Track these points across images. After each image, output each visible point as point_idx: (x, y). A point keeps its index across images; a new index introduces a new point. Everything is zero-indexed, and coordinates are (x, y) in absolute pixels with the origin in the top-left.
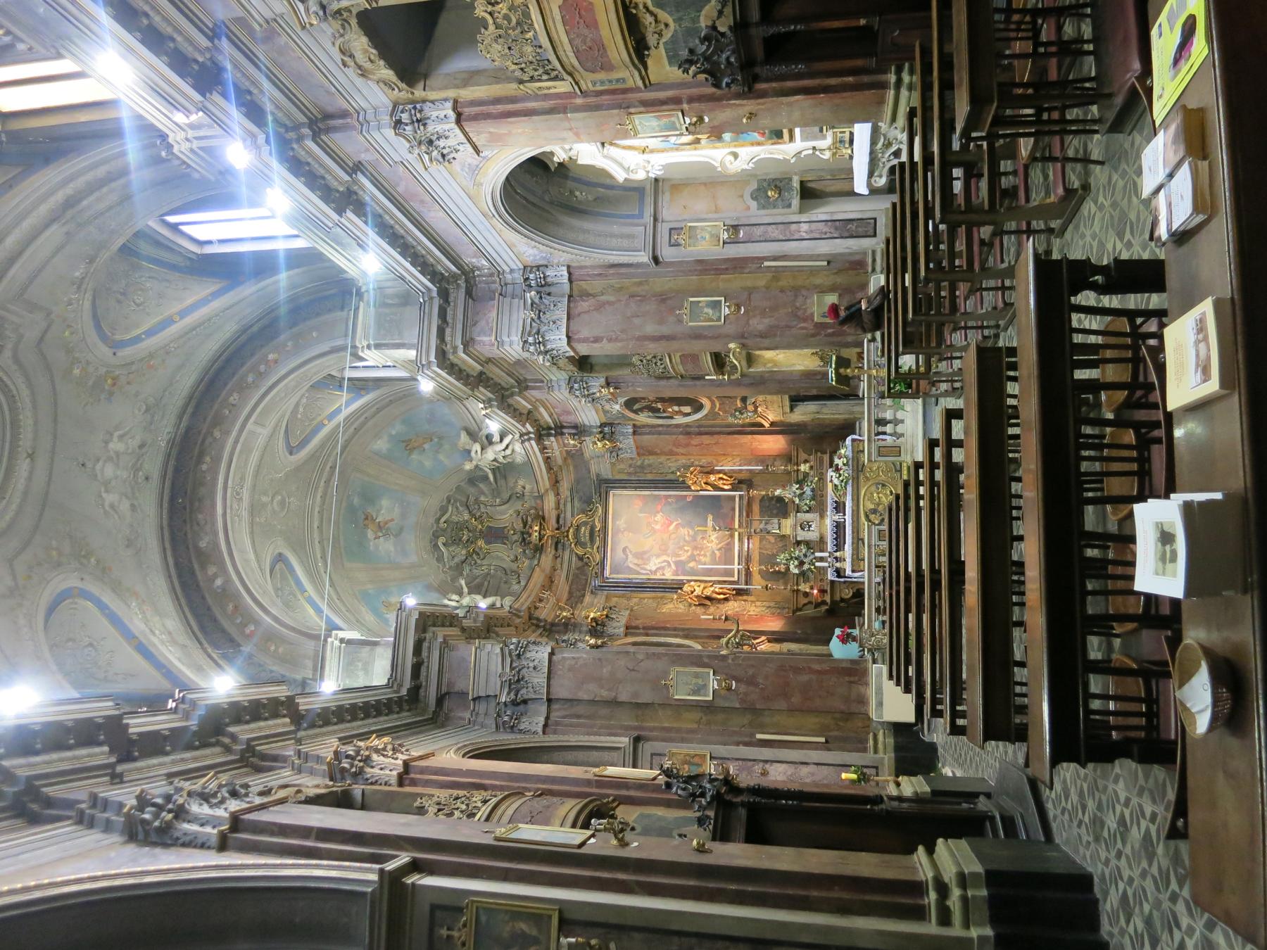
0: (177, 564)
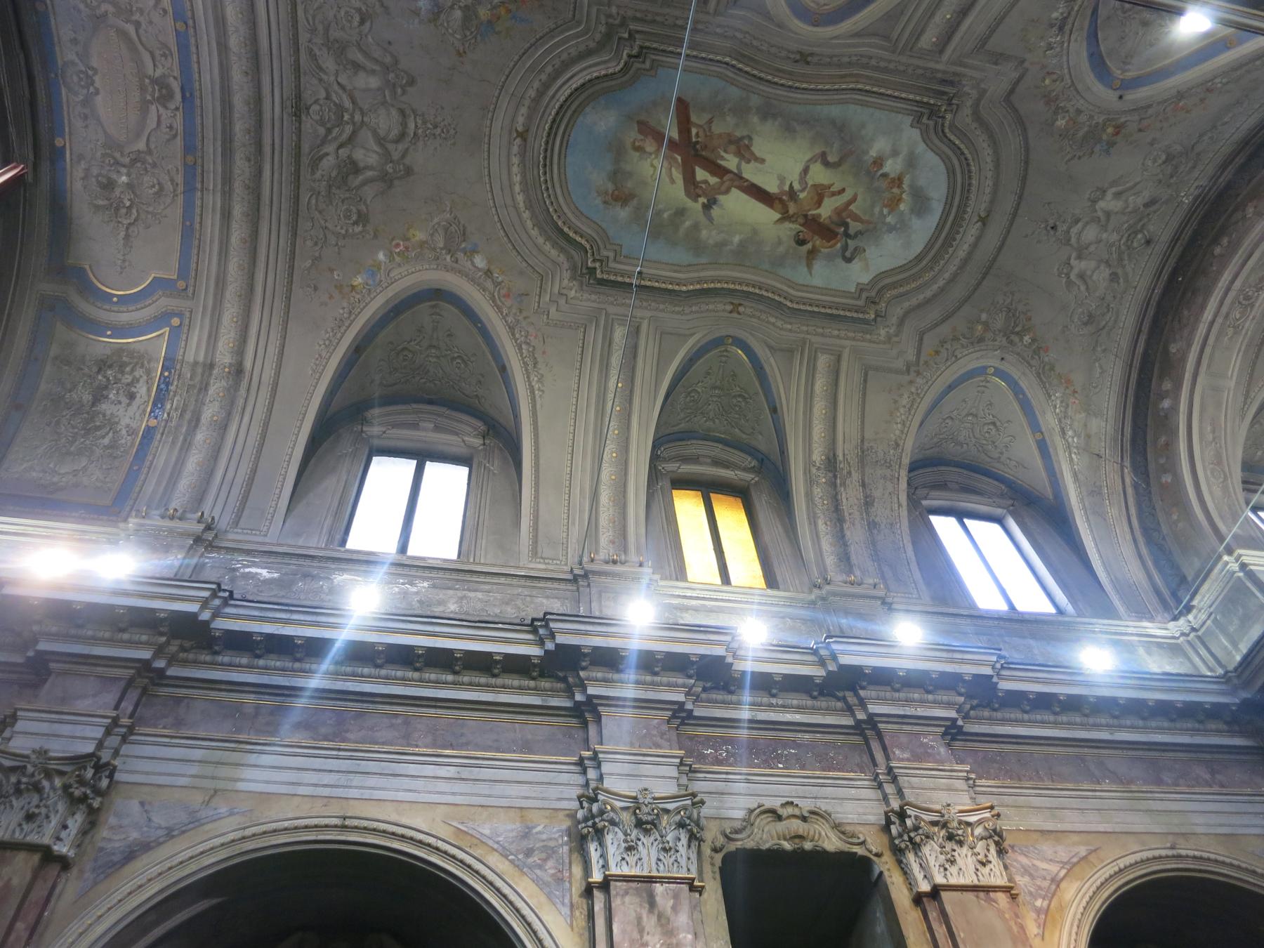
0: (1145, 354)
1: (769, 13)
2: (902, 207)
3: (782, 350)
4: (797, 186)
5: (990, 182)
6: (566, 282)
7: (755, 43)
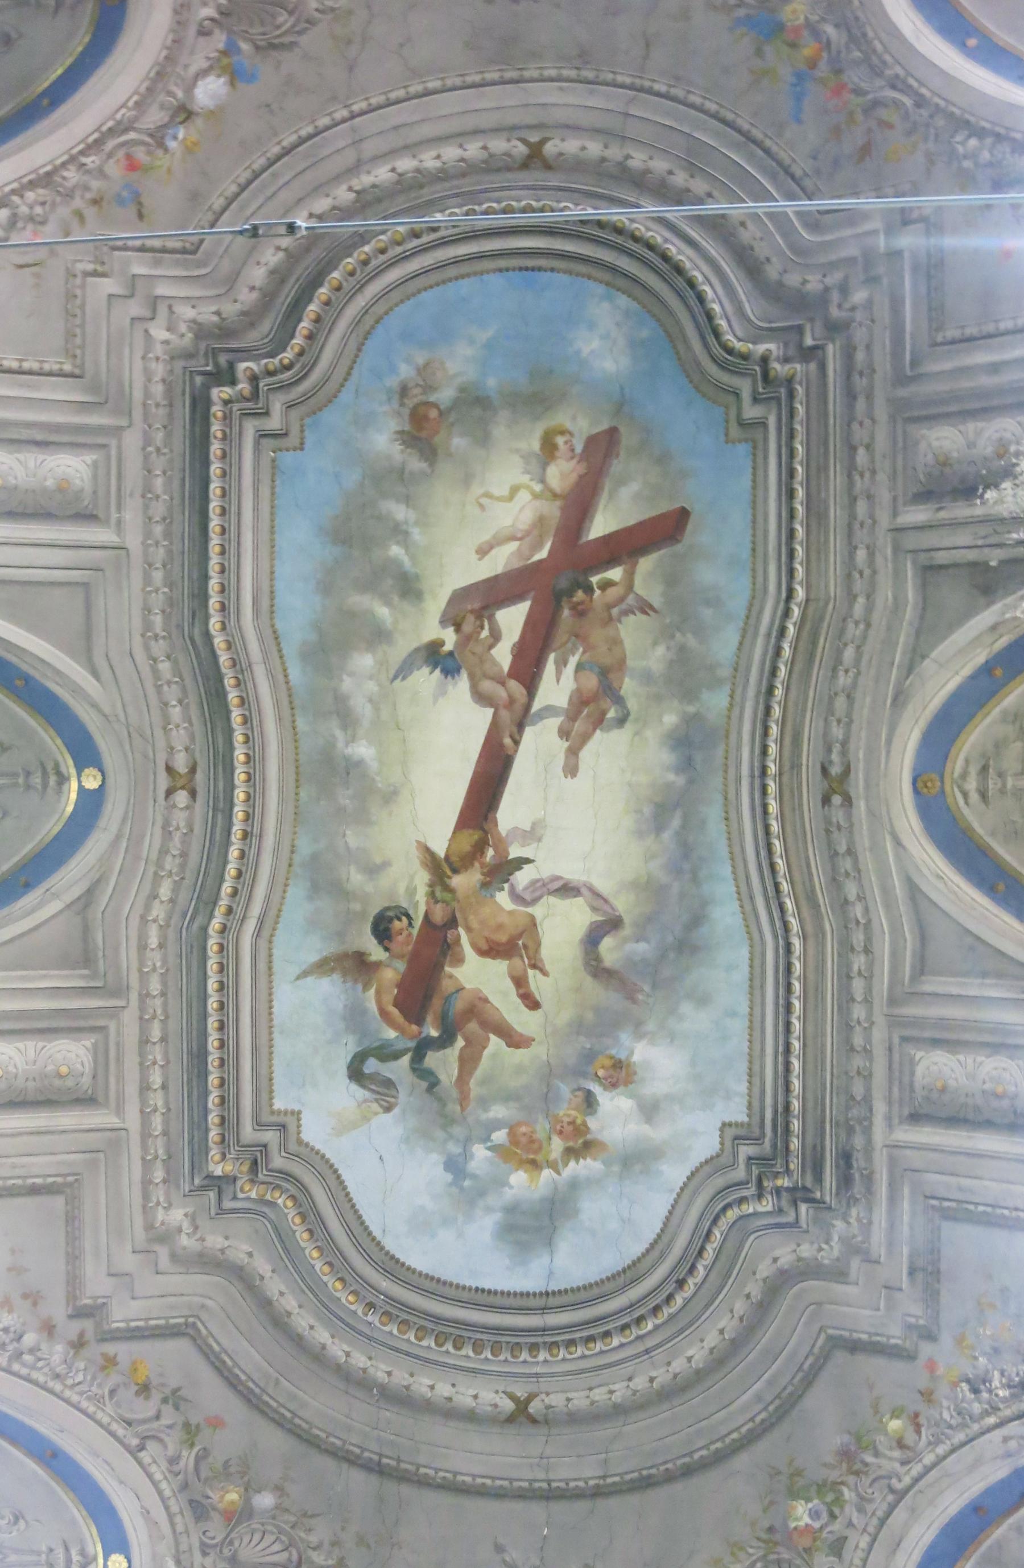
1: (924, 657)
2: (519, 1178)
3: (86, 930)
4: (522, 878)
5: (620, 1392)
6: (187, 312)
7: (849, 654)
